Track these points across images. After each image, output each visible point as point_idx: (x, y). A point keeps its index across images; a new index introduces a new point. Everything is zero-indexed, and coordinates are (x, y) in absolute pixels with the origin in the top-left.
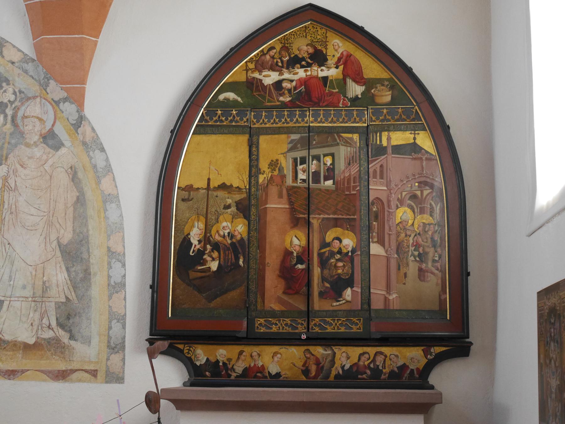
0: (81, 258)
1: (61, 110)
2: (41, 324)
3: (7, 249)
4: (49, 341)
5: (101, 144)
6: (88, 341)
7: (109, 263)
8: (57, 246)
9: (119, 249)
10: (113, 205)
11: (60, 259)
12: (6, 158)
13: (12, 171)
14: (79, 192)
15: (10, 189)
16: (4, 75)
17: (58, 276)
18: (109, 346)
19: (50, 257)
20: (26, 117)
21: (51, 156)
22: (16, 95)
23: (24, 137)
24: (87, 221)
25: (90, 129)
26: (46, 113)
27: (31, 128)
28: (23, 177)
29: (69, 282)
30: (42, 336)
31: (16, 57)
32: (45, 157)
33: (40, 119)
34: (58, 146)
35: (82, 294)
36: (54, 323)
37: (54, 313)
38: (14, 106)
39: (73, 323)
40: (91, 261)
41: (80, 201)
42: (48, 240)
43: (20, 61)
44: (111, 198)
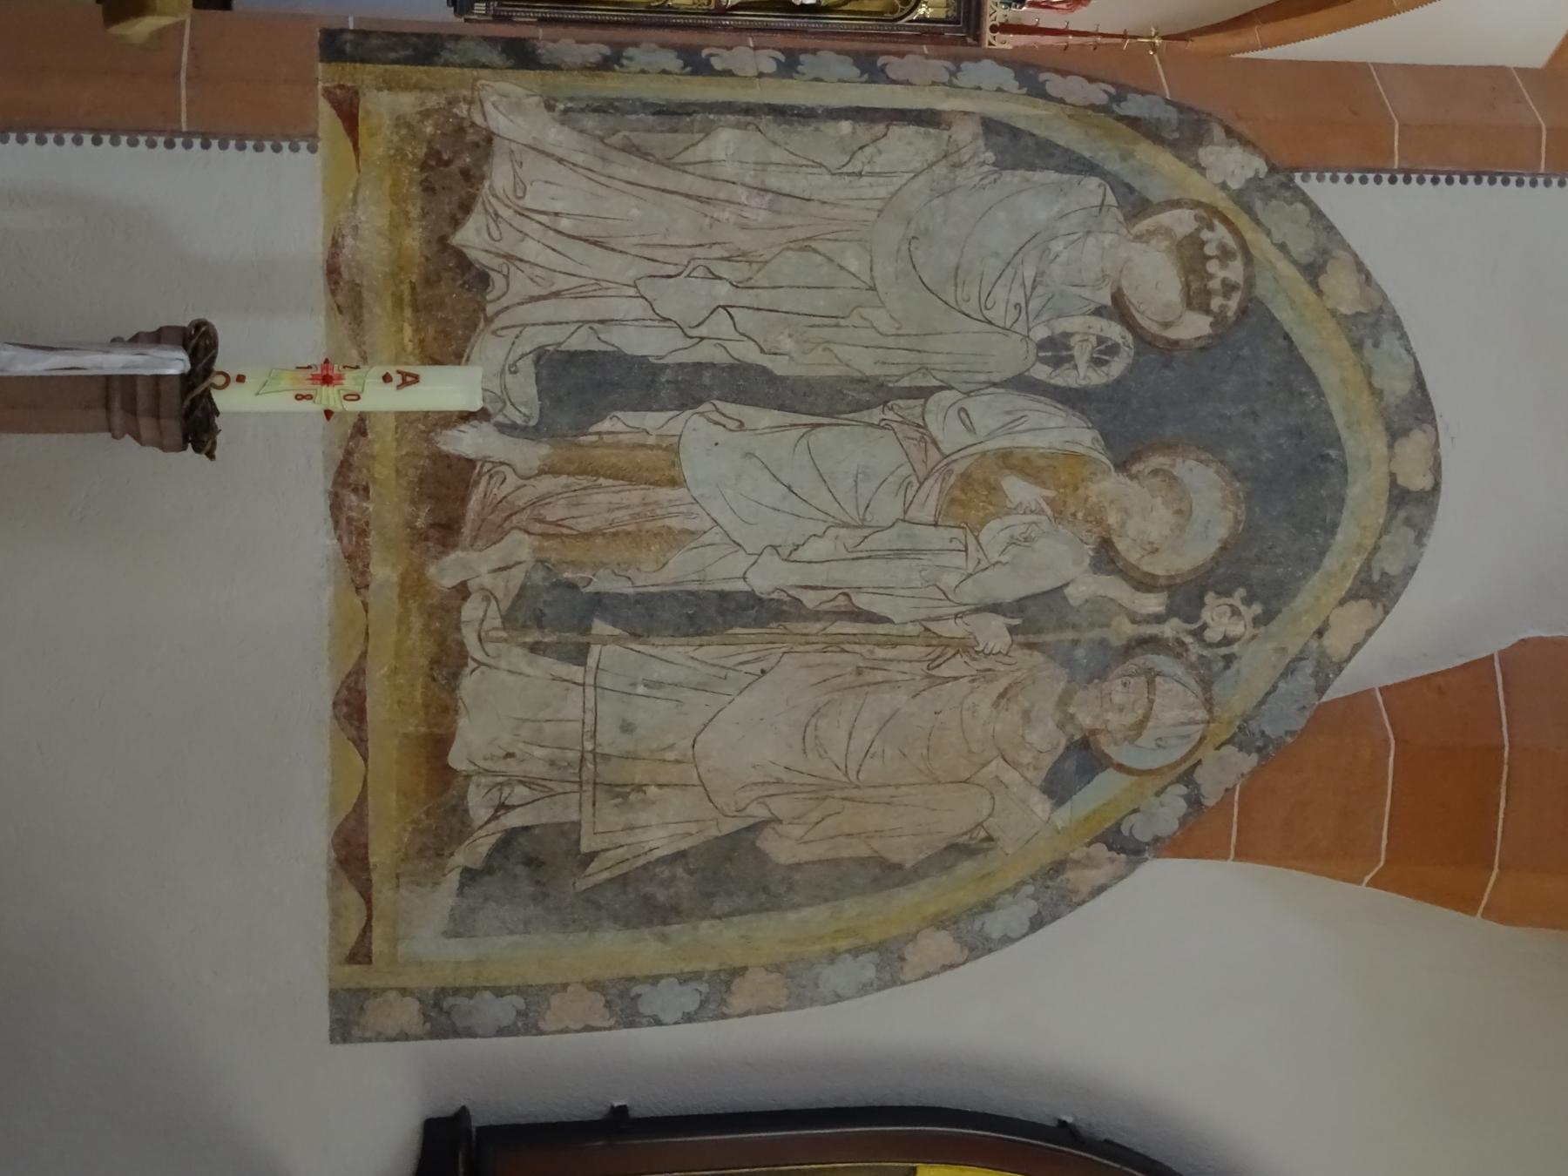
0: (713, 895)
1: (1165, 788)
2: (511, 781)
3: (747, 668)
4: (459, 810)
5: (1055, 918)
6: (459, 927)
7: (697, 976)
8: (751, 821)
9: (738, 1002)
10: (870, 973)
11: (714, 833)
12: (1030, 646)
13: (988, 666)
14: (915, 869)
15: (934, 663)
16: (1285, 610)
17: (661, 829)
18: (442, 992)
19: (719, 801)
20: (1151, 683)
21: (1029, 775)
22: (1219, 644)
23: (1090, 681)
24: (826, 900)
25: (1103, 881)
26: (1160, 744)
27: (1117, 699)
28: (970, 700)
29: (641, 862)
30: (472, 788)
31: (1336, 643)
32: (1026, 758)
33: (1141, 725)
34: (1057, 789)
35: (602, 902)
36: (513, 820)
37: (544, 820)
38: (1188, 639)
39: (515, 877)
40: (705, 924)
41: (886, 874)
42: (773, 790)
43: (1323, 653)
44: (889, 963)
